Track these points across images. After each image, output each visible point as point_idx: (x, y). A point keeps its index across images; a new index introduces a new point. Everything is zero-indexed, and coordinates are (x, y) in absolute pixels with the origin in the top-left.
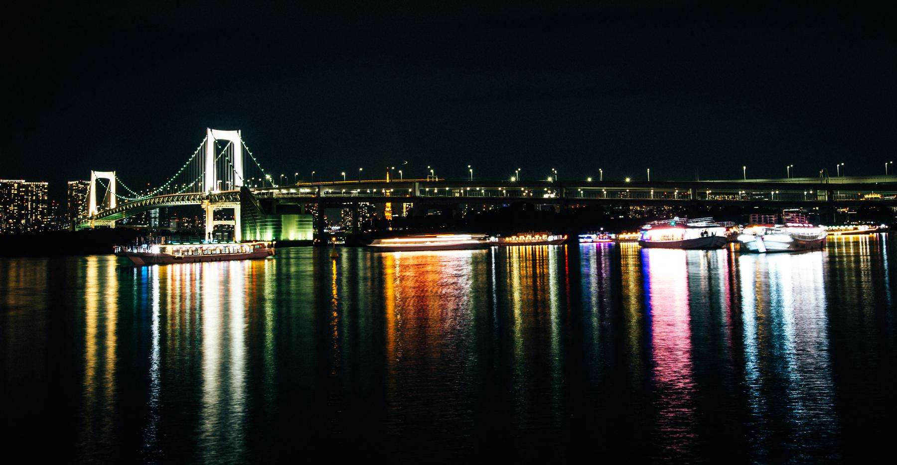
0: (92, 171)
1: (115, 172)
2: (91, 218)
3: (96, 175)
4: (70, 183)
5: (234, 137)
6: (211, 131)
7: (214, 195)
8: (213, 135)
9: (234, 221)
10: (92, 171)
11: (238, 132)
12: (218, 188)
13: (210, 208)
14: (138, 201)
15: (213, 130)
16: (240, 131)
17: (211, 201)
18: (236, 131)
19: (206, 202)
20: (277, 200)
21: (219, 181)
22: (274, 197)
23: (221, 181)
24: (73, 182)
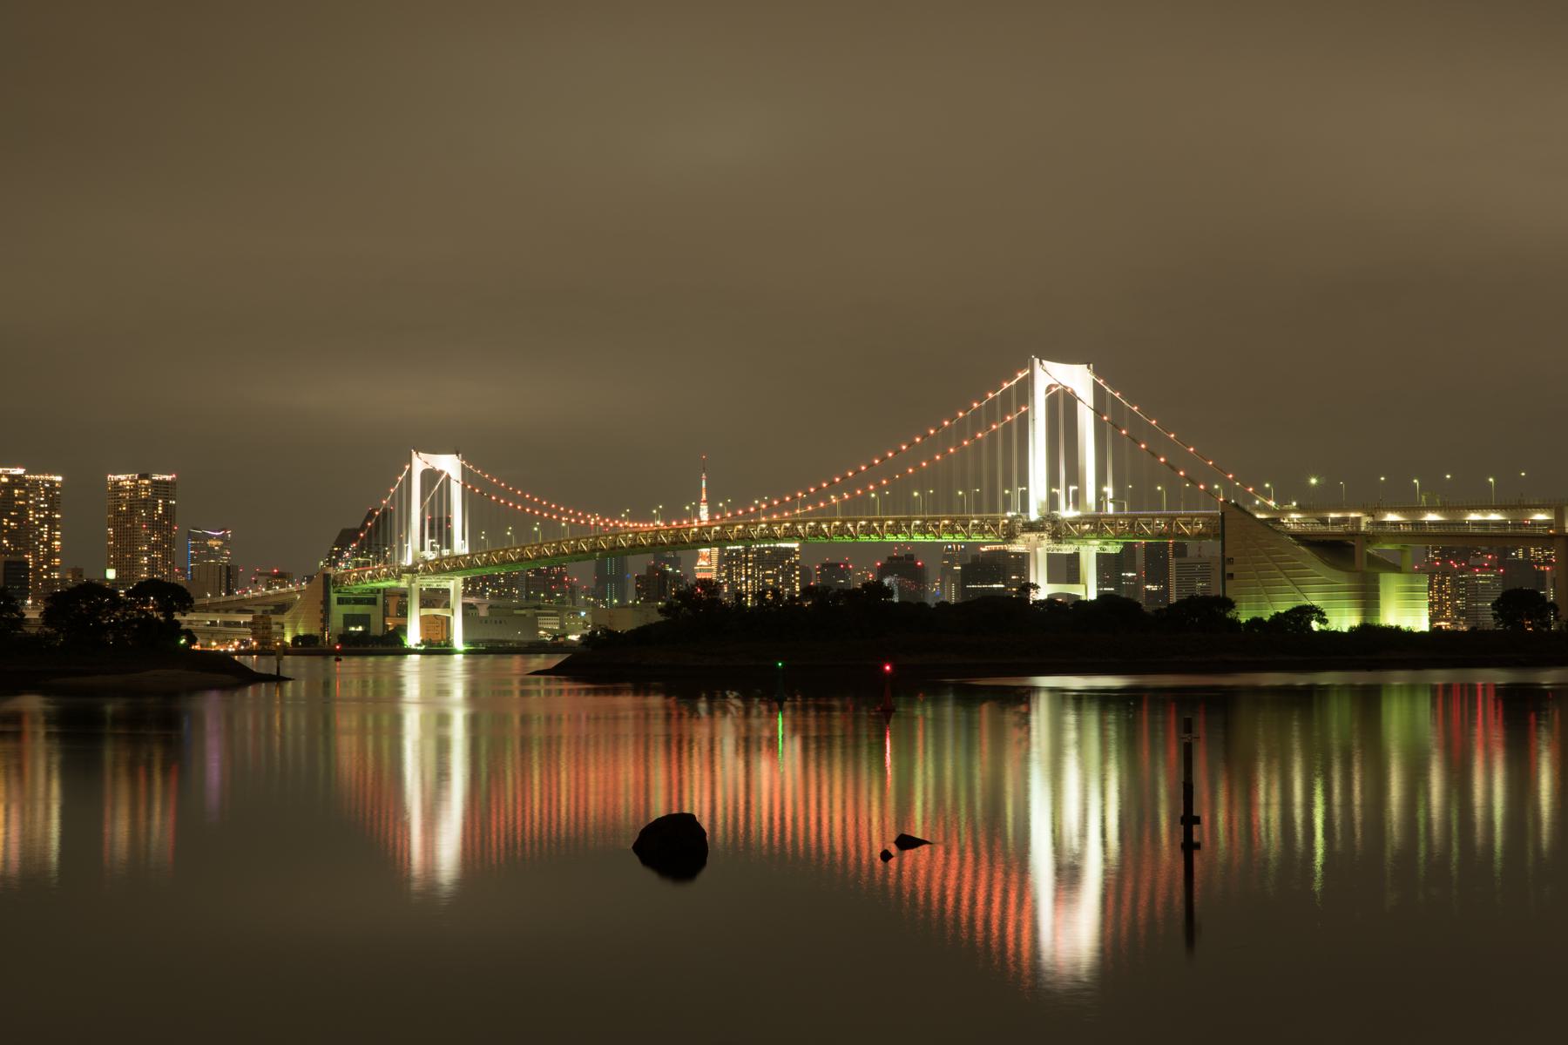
0: (414, 453)
1: (460, 455)
2: (412, 570)
3: (420, 463)
4: (110, 476)
5: (1078, 379)
6: (1041, 363)
7: (1064, 520)
8: (1051, 375)
9: (1083, 586)
10: (414, 453)
11: (1088, 368)
12: (1071, 504)
13: (1038, 549)
14: (657, 531)
15: (1044, 361)
16: (1091, 365)
17: (1056, 537)
18: (1085, 366)
19: (1033, 536)
20: (1370, 538)
21: (1072, 488)
22: (1363, 529)
23: (1076, 488)
24: (122, 477)
